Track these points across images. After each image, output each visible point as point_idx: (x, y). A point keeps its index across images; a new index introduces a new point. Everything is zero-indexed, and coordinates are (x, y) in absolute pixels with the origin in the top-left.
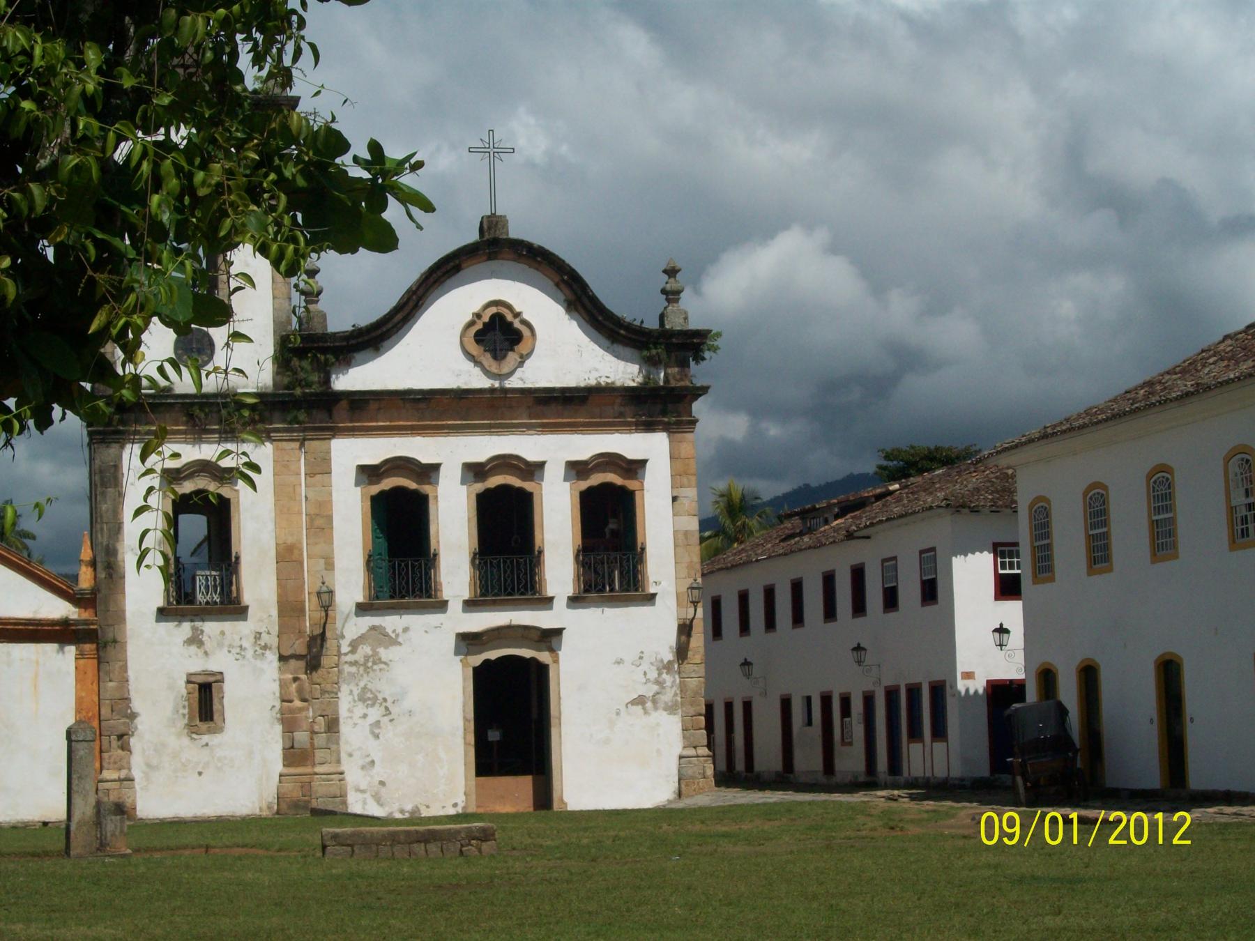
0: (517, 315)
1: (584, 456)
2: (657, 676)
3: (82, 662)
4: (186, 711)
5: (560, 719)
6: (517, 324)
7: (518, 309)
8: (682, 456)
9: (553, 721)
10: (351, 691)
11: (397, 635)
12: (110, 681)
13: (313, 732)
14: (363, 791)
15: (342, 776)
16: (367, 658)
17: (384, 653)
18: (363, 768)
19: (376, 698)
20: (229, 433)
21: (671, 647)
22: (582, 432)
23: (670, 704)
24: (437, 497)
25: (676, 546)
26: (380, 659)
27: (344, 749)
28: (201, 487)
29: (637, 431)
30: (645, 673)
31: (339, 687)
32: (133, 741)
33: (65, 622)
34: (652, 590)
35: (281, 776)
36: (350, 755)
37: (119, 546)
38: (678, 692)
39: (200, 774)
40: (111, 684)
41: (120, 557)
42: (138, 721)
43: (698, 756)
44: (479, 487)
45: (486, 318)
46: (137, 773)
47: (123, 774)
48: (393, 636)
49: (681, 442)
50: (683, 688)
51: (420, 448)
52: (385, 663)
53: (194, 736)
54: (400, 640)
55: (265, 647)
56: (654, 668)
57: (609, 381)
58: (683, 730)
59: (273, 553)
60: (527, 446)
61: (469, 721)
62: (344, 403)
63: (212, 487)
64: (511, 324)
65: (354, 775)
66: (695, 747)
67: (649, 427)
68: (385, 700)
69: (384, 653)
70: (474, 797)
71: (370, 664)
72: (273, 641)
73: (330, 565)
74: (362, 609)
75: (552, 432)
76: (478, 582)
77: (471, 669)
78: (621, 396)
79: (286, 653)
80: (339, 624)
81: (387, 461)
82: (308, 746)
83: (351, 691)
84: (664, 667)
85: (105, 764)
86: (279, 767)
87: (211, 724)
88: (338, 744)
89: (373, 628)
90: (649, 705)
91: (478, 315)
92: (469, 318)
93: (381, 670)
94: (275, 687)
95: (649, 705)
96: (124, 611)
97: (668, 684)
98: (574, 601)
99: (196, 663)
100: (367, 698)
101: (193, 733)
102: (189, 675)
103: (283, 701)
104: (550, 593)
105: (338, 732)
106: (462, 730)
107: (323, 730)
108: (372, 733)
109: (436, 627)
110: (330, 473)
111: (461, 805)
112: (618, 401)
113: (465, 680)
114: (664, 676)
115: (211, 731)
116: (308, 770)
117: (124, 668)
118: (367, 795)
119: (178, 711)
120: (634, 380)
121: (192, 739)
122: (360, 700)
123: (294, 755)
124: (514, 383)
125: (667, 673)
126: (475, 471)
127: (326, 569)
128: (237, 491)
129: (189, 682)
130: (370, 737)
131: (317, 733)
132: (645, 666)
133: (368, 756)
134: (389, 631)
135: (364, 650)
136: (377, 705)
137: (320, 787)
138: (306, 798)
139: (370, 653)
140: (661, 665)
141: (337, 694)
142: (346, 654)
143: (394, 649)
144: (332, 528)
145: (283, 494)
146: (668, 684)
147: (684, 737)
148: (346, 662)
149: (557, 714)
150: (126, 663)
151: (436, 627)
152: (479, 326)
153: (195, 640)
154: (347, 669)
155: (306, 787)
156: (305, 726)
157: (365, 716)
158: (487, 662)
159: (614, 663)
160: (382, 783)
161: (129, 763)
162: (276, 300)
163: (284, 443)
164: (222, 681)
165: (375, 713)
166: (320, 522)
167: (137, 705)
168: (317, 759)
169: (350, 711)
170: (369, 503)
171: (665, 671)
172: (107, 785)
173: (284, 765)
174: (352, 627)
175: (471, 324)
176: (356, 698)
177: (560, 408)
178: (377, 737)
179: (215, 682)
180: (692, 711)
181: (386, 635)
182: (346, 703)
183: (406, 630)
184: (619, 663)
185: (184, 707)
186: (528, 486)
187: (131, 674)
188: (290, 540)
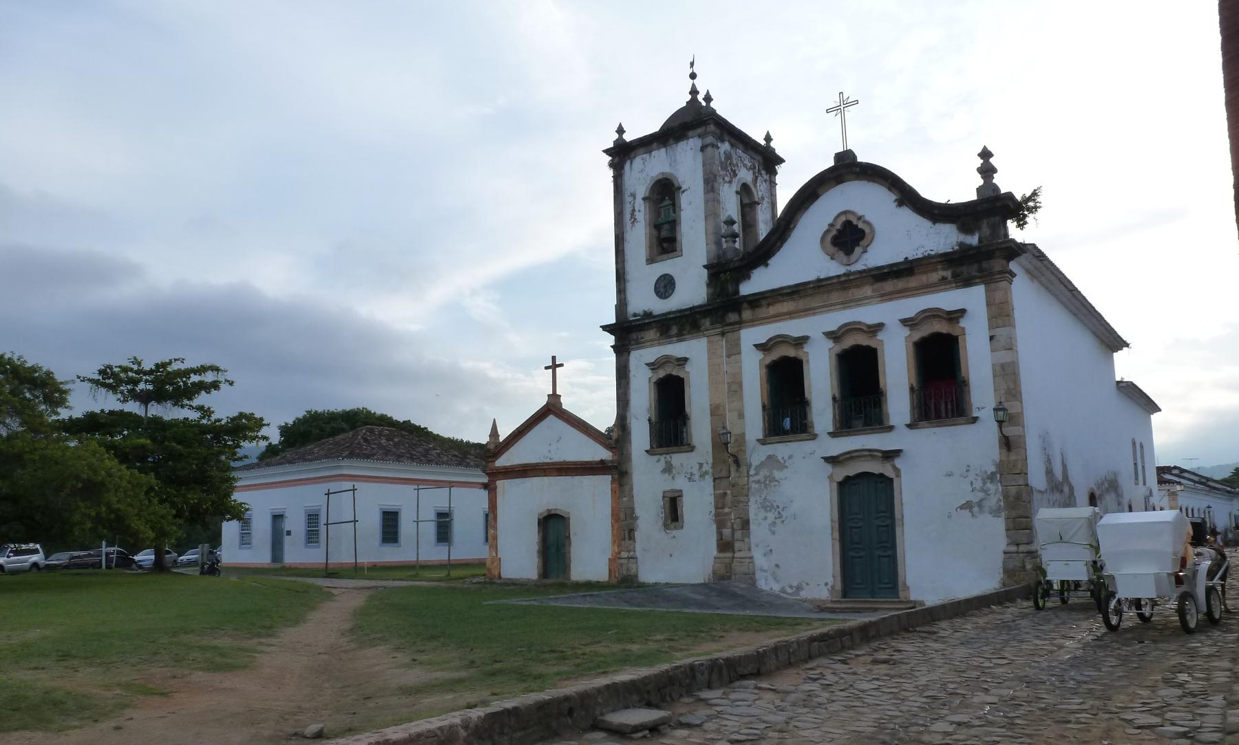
0: (860, 218)
1: (910, 314)
2: (982, 485)
3: (614, 486)
4: (663, 515)
5: (902, 521)
6: (861, 225)
7: (860, 213)
8: (997, 301)
9: (898, 523)
10: (757, 501)
11: (785, 461)
12: (625, 497)
13: (732, 528)
14: (764, 571)
15: (750, 560)
16: (766, 478)
17: (777, 474)
18: (765, 555)
19: (772, 505)
20: (681, 337)
21: (993, 461)
22: (913, 296)
23: (994, 508)
24: (808, 361)
25: (994, 376)
26: (774, 478)
27: (754, 539)
28: (668, 373)
29: (957, 287)
30: (972, 483)
31: (749, 499)
32: (637, 534)
33: (602, 462)
34: (975, 415)
35: (715, 558)
36: (757, 546)
37: (628, 415)
38: (1001, 498)
39: (671, 555)
40: (625, 499)
41: (628, 422)
42: (638, 521)
43: (1018, 553)
44: (839, 348)
45: (838, 226)
46: (638, 554)
47: (632, 553)
48: (782, 461)
49: (994, 291)
50: (1006, 496)
51: (793, 328)
52: (777, 481)
53: (667, 531)
54: (786, 464)
55: (706, 473)
56: (979, 478)
57: (933, 253)
58: (1006, 530)
59: (708, 411)
60: (868, 314)
61: (834, 522)
62: (745, 305)
63: (674, 373)
64: (857, 226)
65: (760, 560)
66: (1018, 545)
67: (967, 282)
68: (778, 507)
69: (777, 474)
70: (839, 579)
71: (768, 482)
72: (707, 467)
73: (741, 415)
74: (763, 442)
75: (890, 300)
76: (837, 417)
77: (835, 483)
78: (939, 262)
79: (715, 477)
80: (748, 456)
81: (770, 340)
82: (730, 539)
83: (757, 501)
84: (988, 478)
85: (623, 549)
86: (715, 552)
87: (677, 524)
88: (749, 537)
89: (769, 457)
90: (976, 509)
91: (831, 225)
92: (826, 227)
93: (775, 486)
94: (712, 499)
95: (976, 509)
96: (631, 454)
97: (992, 491)
98: (910, 426)
99: (668, 484)
100: (767, 506)
101: (667, 529)
102: (664, 492)
103: (716, 508)
104: (891, 424)
105: (749, 529)
106: (830, 529)
107: (739, 528)
108: (770, 530)
109: (811, 454)
110: (740, 353)
111: (830, 584)
112: (939, 267)
113: (831, 491)
114: (989, 485)
115: (676, 528)
116: (729, 555)
117: (631, 489)
118: (766, 574)
119: (659, 516)
120: (953, 248)
121: (666, 533)
122: (762, 507)
123: (725, 545)
124: (859, 267)
125: (991, 483)
126: (834, 336)
127: (739, 418)
128: (689, 373)
129: (664, 497)
130: (769, 533)
131: (736, 530)
132: (971, 477)
133: (768, 546)
134: (780, 458)
135: (764, 472)
136: (773, 510)
137: (738, 568)
138: (728, 574)
139: (768, 474)
140: (985, 476)
141: (747, 503)
142: (753, 476)
143: (785, 470)
144: (742, 390)
145: (714, 370)
146: (992, 491)
147: (1007, 536)
148: (753, 481)
149: (900, 517)
150: (632, 485)
151: (811, 454)
152: (834, 233)
153: (668, 469)
154: (754, 486)
155: (729, 567)
156: (729, 524)
157: (766, 518)
158: (848, 478)
159: (946, 476)
160: (777, 566)
161: (635, 548)
162: (709, 246)
163: (712, 337)
164: (681, 496)
165: (771, 516)
166: (734, 387)
167: (638, 512)
168: (736, 549)
169: (756, 515)
170: (764, 370)
171: (989, 481)
172: (622, 561)
173: (717, 551)
174: (757, 455)
175: (827, 232)
176: (760, 506)
177: (895, 281)
178: (773, 533)
179: (679, 496)
180: (1014, 514)
181: (778, 461)
182: (754, 511)
183: (790, 457)
184: (949, 475)
185: (662, 512)
186: (872, 343)
187: (634, 491)
188: (717, 402)
